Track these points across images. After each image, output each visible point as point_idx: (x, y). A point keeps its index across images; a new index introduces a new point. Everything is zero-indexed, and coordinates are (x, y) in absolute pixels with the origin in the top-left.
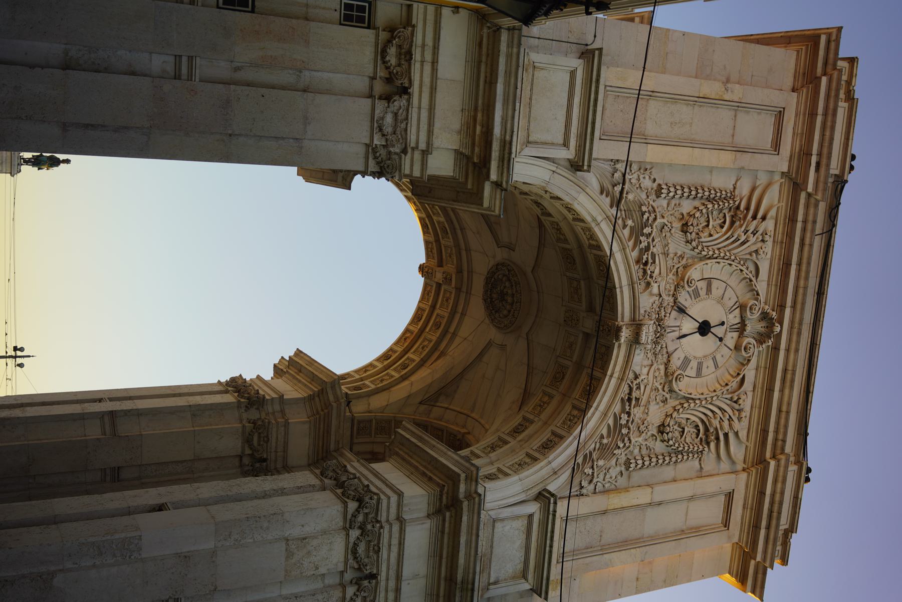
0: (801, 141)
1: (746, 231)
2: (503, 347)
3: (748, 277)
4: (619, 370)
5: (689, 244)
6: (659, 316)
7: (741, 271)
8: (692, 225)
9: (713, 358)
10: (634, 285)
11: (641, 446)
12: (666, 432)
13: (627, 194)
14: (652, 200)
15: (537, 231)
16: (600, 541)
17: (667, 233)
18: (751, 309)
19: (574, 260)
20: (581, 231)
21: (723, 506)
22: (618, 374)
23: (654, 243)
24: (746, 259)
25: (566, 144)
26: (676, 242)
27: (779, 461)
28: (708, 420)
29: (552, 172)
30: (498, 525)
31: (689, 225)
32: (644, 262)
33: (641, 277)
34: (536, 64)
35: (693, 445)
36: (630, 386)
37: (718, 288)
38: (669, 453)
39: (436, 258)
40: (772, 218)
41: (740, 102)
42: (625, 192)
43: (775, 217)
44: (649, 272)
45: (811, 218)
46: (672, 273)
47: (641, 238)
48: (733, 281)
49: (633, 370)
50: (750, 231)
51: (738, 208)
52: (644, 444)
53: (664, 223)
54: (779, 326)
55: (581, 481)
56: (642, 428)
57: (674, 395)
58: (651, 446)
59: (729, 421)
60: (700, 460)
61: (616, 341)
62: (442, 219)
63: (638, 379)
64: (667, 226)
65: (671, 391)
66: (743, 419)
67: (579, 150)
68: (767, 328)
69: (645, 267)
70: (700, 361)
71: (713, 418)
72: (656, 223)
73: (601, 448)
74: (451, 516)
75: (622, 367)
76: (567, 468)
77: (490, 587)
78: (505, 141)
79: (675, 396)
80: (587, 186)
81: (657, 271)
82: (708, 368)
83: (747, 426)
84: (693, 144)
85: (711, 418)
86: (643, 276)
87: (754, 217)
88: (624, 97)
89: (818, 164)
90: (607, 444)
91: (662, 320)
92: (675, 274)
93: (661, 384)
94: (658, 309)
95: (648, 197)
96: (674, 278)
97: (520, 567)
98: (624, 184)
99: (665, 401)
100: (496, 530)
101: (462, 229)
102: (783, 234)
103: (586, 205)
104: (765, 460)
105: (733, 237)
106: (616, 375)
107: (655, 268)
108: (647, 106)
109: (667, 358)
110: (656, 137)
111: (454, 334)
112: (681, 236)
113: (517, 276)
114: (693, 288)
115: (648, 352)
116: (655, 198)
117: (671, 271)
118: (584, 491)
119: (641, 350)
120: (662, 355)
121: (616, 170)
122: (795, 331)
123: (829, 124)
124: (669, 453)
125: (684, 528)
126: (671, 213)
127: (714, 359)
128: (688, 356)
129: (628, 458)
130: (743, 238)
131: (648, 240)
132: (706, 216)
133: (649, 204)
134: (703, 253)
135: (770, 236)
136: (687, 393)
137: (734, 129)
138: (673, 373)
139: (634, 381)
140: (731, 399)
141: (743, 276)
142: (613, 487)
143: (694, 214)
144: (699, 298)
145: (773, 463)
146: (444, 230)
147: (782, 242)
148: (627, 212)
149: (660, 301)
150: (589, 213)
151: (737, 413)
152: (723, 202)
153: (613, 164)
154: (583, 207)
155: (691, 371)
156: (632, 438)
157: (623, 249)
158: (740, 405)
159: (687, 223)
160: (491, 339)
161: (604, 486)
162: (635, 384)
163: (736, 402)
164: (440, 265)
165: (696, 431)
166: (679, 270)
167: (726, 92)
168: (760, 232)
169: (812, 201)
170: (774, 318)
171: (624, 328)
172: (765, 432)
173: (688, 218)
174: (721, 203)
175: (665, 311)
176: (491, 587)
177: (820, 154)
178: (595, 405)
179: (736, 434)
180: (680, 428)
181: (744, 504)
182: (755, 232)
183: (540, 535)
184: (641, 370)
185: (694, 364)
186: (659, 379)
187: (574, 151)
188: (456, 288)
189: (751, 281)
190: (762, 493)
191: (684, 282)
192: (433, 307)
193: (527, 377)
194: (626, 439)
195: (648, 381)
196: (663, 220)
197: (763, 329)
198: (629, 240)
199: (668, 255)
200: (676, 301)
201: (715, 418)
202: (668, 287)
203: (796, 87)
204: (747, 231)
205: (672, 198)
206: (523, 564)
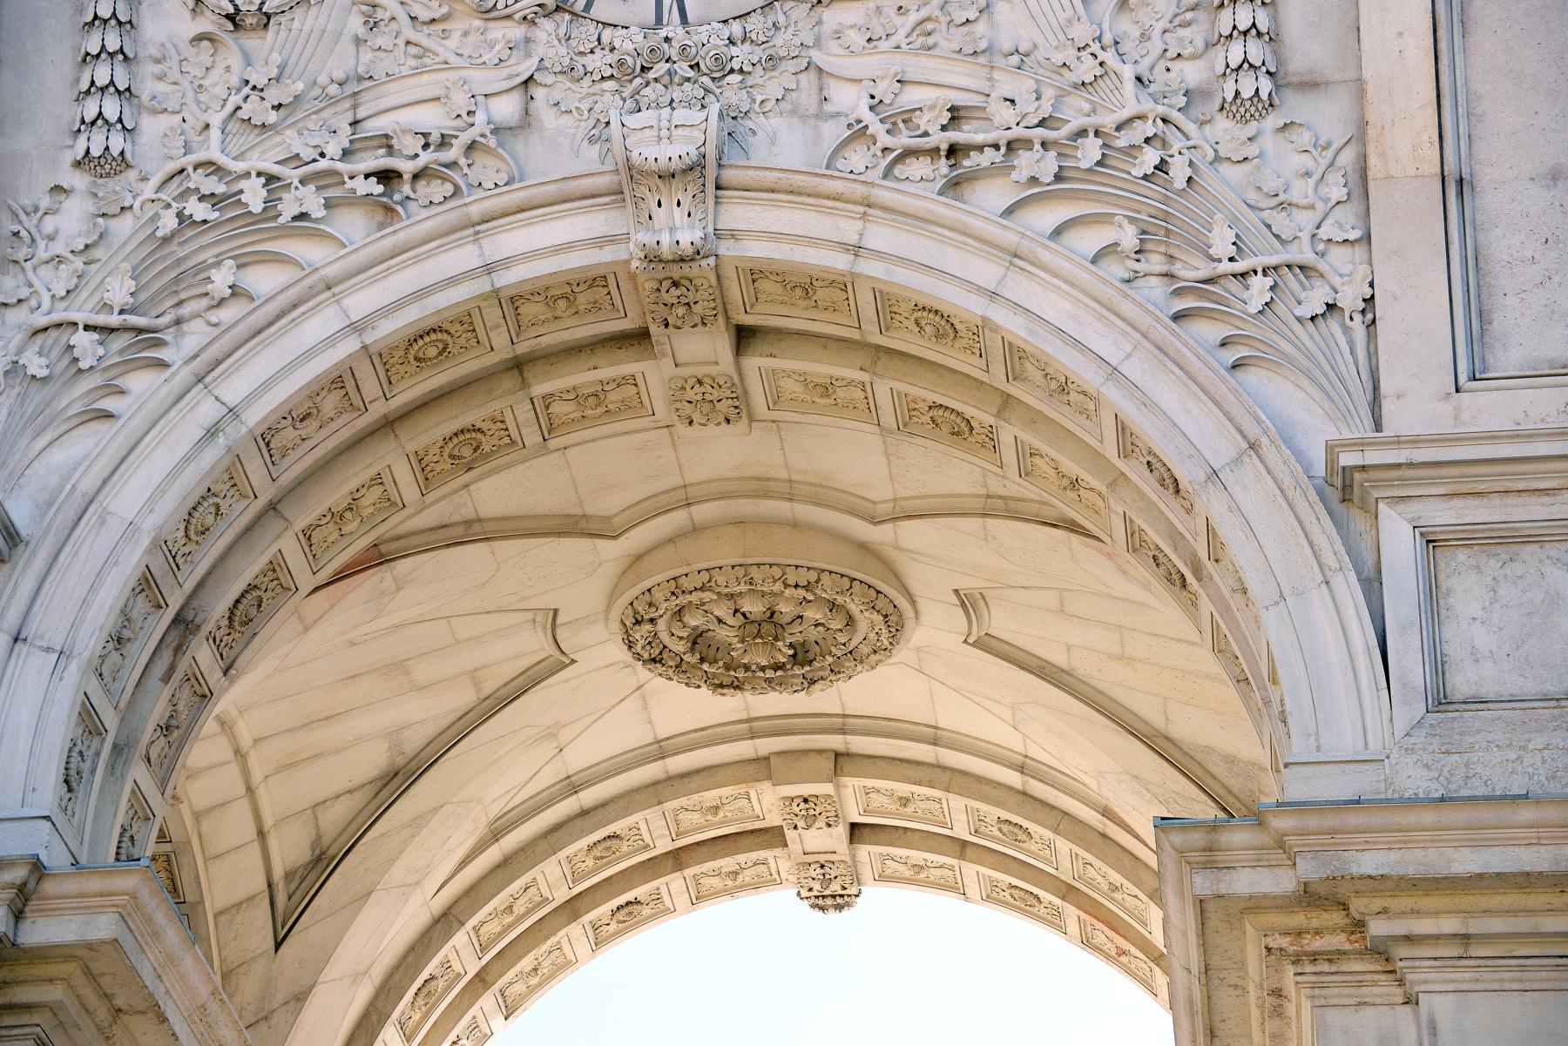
2: (968, 603)
10: (476, 218)
20: (293, 456)
29: (19, 644)
31: (231, 10)
32: (380, 189)
36: (900, 158)
39: (762, 854)
42: (102, 319)
44: (426, 158)
47: (281, 220)
49: (828, 167)
52: (1156, 46)
53: (226, 122)
56: (1086, 69)
63: (870, 131)
64: (239, 108)
69: (407, 177)
72: (223, 160)
74: (1385, 911)
75: (820, 210)
81: (432, 119)
86: (444, 179)
91: (621, 63)
92: (438, 27)
100: (1489, 691)
101: (572, 786)
106: (849, 230)
112: (283, 34)
115: (759, 98)
116: (132, 175)
117: (426, 50)
119: (754, 133)
126: (190, 94)
129: (1222, 109)
131: (296, 183)
139: (879, 144)
142: (1347, 158)
148: (183, 296)
150: (187, 460)
154: (161, 489)
156: (1125, 114)
159: (228, 17)
160: (965, 641)
162: (884, 140)
164: (772, 837)
166: (425, 15)
173: (209, 13)
184: (837, 115)
188: (837, 771)
192: (962, 848)
193: (1027, 520)
196: (215, 133)
199: (360, 79)
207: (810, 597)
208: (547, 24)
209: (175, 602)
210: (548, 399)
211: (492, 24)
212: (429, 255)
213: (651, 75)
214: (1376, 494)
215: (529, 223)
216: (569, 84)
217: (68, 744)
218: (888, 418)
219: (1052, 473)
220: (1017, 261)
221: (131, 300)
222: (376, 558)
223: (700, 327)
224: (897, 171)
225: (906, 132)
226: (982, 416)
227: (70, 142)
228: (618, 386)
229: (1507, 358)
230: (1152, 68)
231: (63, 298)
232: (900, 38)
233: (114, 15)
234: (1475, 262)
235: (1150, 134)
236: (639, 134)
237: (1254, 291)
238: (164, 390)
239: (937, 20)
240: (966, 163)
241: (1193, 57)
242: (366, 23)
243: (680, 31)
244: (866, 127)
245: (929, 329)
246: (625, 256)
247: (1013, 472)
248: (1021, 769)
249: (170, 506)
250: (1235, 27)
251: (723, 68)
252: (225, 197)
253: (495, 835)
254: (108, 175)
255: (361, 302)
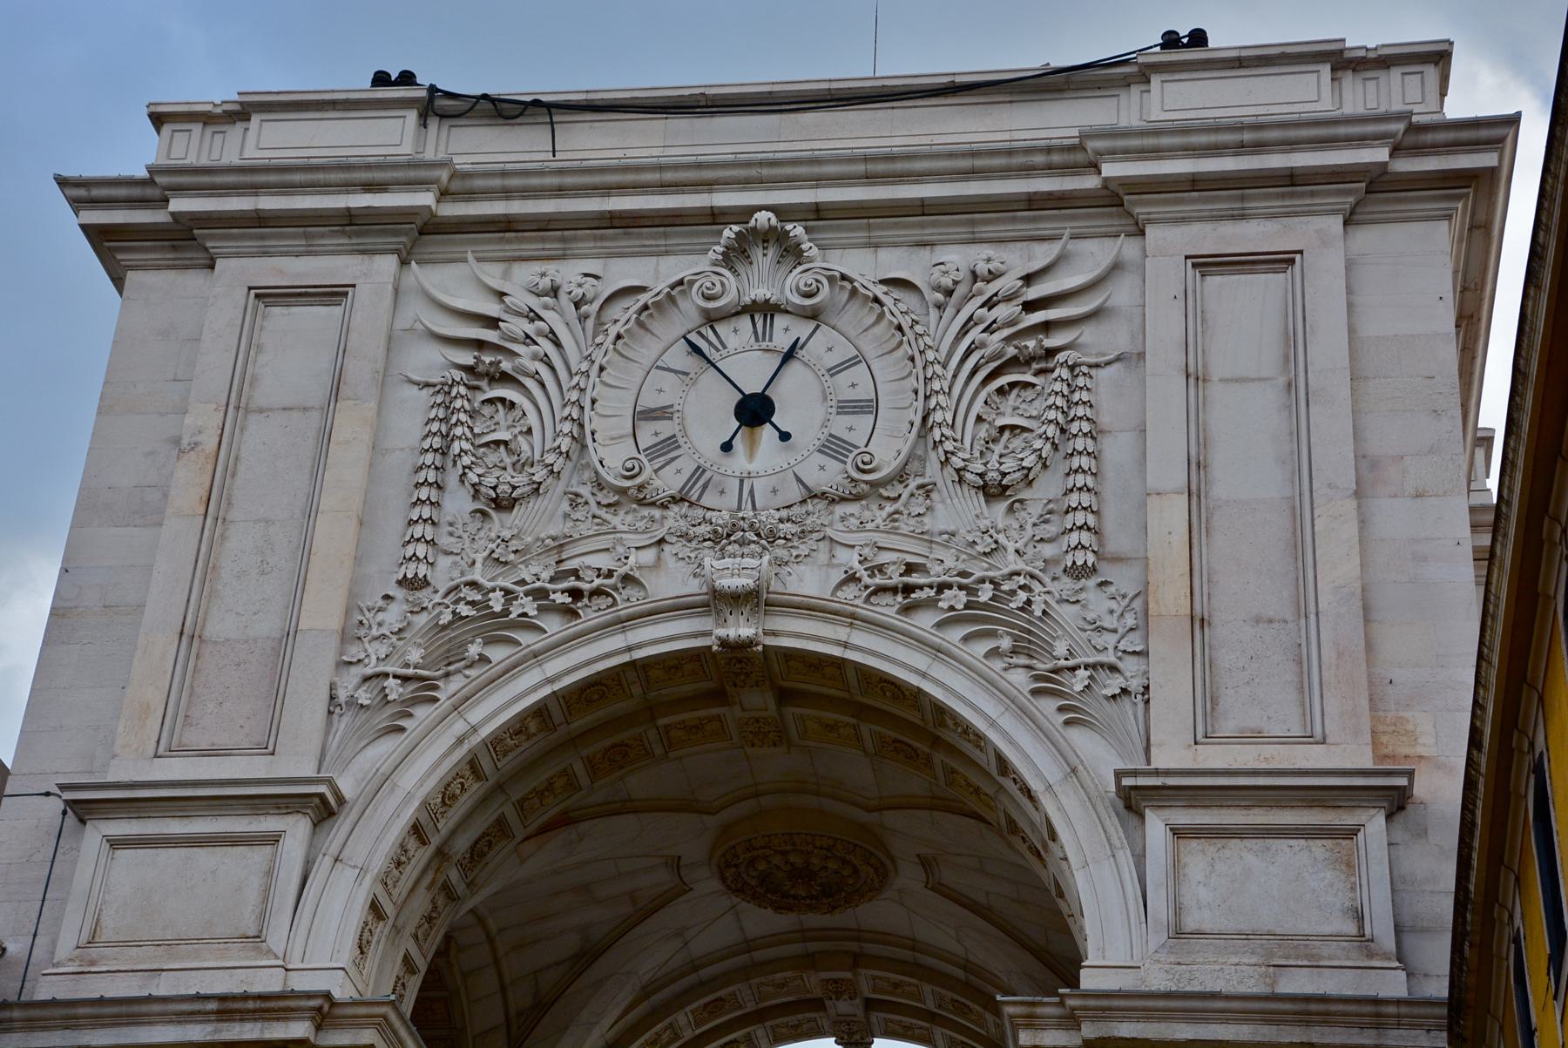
0: (323, 236)
1: (528, 340)
2: (926, 863)
3: (635, 316)
4: (830, 627)
5: (542, 487)
6: (709, 539)
7: (619, 337)
8: (494, 488)
9: (832, 375)
10: (624, 619)
11: (1035, 538)
12: (1000, 478)
13: (407, 666)
14: (432, 596)
15: (583, 826)
16: (1286, 622)
17: (510, 549)
18: (709, 298)
19: (614, 746)
20: (511, 756)
21: (1237, 277)
22: (839, 629)
23: (528, 579)
24: (599, 323)
25: (274, 839)
26: (535, 522)
27: (1099, 153)
28: (987, 362)
29: (338, 863)
30: (1190, 923)
32: (570, 599)
33: (610, 599)
34: (85, 937)
35: (1050, 395)
36: (875, 593)
37: (660, 391)
38: (1065, 458)
39: (813, 1015)
40: (506, 276)
41: (227, 405)
43: (507, 264)
44: (598, 582)
45: (497, 182)
46: (608, 517)
47: (511, 616)
48: (646, 351)
49: (832, 595)
50: (530, 328)
51: (469, 370)
52: (1029, 531)
53: (485, 559)
54: (756, 216)
55: (1107, 698)
57: (914, 466)
58: (1040, 512)
59: (999, 302)
60: (1097, 366)
61: (757, 645)
62: (681, 1018)
63: (858, 575)
64: (493, 551)
65: (902, 476)
66: (991, 266)
67: (287, 807)
68: (767, 241)
70: (834, 410)
71: (983, 351)
72: (482, 581)
73: (1026, 651)
75: (826, 621)
76: (1061, 740)
77: (1366, 932)
78: (218, 1012)
79: (916, 463)
80: (378, 770)
81: (604, 562)
82: (855, 383)
83: (1025, 244)
84: (311, 512)
85: (983, 357)
86: (608, 595)
87: (492, 323)
88: (189, 702)
89: (370, 187)
90: (1016, 638)
91: (715, 532)
93: (881, 508)
94: (694, 543)
95: (423, 609)
96: (622, 513)
97: (1319, 848)
98: (386, 675)
99: (927, 490)
100: (1207, 927)
101: (693, 966)
102: (543, 240)
103: (425, 768)
104: (1105, 187)
105: (537, 373)
106: (842, 633)
107: (589, 567)
108: (216, 642)
109: (816, 501)
110: (288, 608)
111: (967, 966)
112: (522, 510)
113: (734, 847)
114: (645, 460)
115: (795, 554)
116: (430, 589)
117: (605, 521)
118: (1135, 685)
119: (790, 574)
120: (808, 513)
121: (352, 702)
122: (765, 172)
123: (273, 178)
124: (1065, 458)
125: (1282, 380)
126: (467, 541)
127: (833, 371)
128: (818, 443)
129: (1065, 571)
130: (546, 346)
131: (522, 595)
132: (482, 450)
133: (440, 604)
134: (564, 449)
135: (543, 275)
136: (907, 434)
137: (291, 409)
138: (853, 480)
140: (940, 307)
141: (636, 329)
142: (1137, 604)
143: (473, 485)
144: (679, 435)
145: (1110, 170)
146: (715, 1007)
147: (563, 240)
148: (451, 659)
149: (674, 539)
150: (446, 755)
151: (979, 284)
152: (453, 413)
153: (338, 710)
154: (429, 774)
155: (855, 429)
156: (1006, 571)
157: (536, 657)
158: (956, 283)
159: (493, 500)
160: (926, 887)
161: (1132, 629)
162: (867, 580)
163: (949, 293)
164: (817, 1005)
165: (1015, 392)
166: (604, 502)
167: (200, 448)
168: (534, 303)
169: (456, 185)
170: (736, 233)
171: (721, 632)
172: (1033, 202)
174: (453, 421)
175: (700, 524)
176: (1368, 931)
177: (348, 187)
178: (914, 680)
179: (1028, 279)
180: (1002, 435)
181: (1233, 218)
182: (532, 314)
183: (1229, 803)
185: (840, 425)
186: (867, 515)
187: (290, 816)
189: (646, 307)
190: (1195, 183)
191: (629, 488)
192: (932, 1017)
194: (1005, 587)
195: (867, 545)
196: (478, 565)
197: (771, 252)
198: (517, 643)
200: (678, 498)
201: (983, 345)
202: (641, 525)
203: (208, 262)
204: (528, 336)
205: (435, 544)
206: (1311, 842)
207: (830, 855)
208: (675, 508)
209: (435, 841)
210: (668, 727)
211: (642, 508)
212: (596, 639)
213: (732, 538)
214: (1143, 804)
215: (655, 623)
216: (684, 542)
217: (362, 924)
218: (869, 745)
219: (963, 783)
220: (939, 654)
221: (421, 661)
222: (564, 821)
223: (755, 688)
224: (872, 599)
225: (878, 576)
226: (923, 747)
227: (397, 570)
228: (710, 721)
229: (1228, 726)
230: (1026, 545)
231: (383, 660)
232: (879, 521)
233: (428, 498)
234: (1210, 665)
235: (1022, 583)
236: (721, 573)
237: (1079, 678)
238: (435, 714)
239: (901, 513)
240: (913, 596)
241: (1050, 540)
242: (571, 505)
243: (751, 513)
244: (856, 573)
245: (888, 693)
246: (709, 643)
247: (942, 783)
248: (964, 968)
249: (431, 783)
250: (1074, 524)
251: (772, 537)
252: (479, 603)
253: (646, 992)
254: (416, 589)
255: (554, 666)
